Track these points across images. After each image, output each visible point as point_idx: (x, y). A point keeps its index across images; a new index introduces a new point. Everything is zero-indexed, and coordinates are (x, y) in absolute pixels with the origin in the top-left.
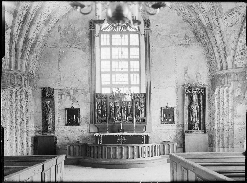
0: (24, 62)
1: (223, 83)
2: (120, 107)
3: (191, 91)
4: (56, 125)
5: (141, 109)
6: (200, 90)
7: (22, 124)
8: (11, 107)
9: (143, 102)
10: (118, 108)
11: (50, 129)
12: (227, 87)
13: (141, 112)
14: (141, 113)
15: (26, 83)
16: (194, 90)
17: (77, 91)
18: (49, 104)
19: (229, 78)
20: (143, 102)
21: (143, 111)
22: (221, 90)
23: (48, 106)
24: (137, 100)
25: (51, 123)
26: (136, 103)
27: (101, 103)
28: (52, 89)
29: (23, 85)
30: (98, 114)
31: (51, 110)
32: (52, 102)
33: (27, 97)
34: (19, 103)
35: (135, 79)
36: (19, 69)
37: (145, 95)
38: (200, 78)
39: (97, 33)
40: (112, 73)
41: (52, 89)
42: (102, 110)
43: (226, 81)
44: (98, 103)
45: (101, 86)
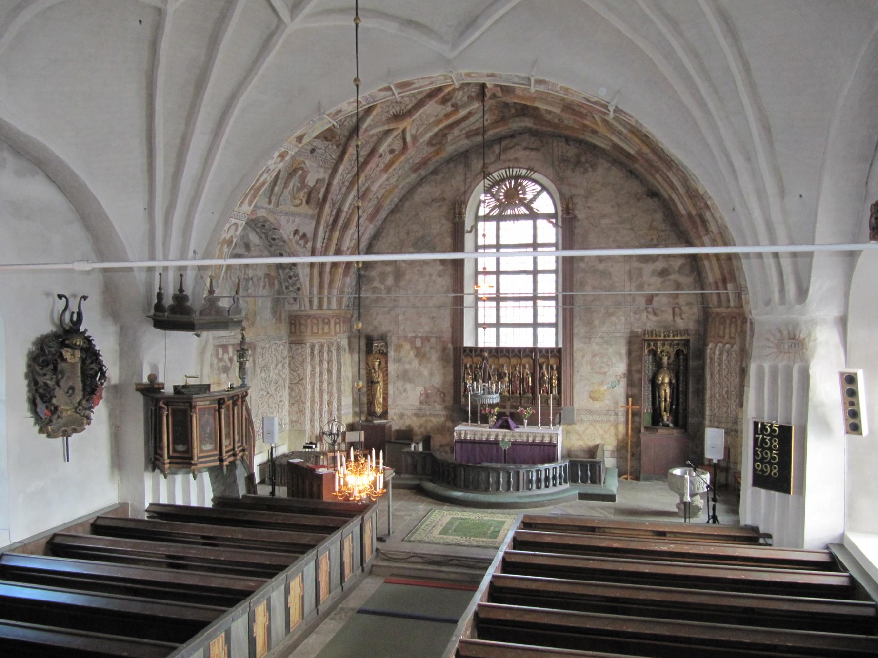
0: (335, 292)
1: (721, 333)
3: (656, 345)
4: (390, 402)
5: (551, 379)
6: (678, 344)
7: (330, 403)
8: (313, 375)
9: (555, 367)
11: (379, 410)
12: (728, 346)
13: (551, 385)
15: (338, 330)
16: (664, 345)
17: (429, 341)
18: (380, 364)
19: (733, 326)
20: (555, 367)
21: (555, 382)
22: (718, 348)
23: (376, 367)
24: (542, 360)
25: (381, 400)
26: (541, 368)
27: (471, 366)
28: (383, 338)
29: (333, 333)
31: (381, 375)
33: (338, 354)
34: (325, 365)
35: (548, 312)
36: (325, 306)
38: (681, 315)
39: (467, 227)
40: (498, 299)
41: (383, 338)
43: (727, 331)
44: (466, 366)
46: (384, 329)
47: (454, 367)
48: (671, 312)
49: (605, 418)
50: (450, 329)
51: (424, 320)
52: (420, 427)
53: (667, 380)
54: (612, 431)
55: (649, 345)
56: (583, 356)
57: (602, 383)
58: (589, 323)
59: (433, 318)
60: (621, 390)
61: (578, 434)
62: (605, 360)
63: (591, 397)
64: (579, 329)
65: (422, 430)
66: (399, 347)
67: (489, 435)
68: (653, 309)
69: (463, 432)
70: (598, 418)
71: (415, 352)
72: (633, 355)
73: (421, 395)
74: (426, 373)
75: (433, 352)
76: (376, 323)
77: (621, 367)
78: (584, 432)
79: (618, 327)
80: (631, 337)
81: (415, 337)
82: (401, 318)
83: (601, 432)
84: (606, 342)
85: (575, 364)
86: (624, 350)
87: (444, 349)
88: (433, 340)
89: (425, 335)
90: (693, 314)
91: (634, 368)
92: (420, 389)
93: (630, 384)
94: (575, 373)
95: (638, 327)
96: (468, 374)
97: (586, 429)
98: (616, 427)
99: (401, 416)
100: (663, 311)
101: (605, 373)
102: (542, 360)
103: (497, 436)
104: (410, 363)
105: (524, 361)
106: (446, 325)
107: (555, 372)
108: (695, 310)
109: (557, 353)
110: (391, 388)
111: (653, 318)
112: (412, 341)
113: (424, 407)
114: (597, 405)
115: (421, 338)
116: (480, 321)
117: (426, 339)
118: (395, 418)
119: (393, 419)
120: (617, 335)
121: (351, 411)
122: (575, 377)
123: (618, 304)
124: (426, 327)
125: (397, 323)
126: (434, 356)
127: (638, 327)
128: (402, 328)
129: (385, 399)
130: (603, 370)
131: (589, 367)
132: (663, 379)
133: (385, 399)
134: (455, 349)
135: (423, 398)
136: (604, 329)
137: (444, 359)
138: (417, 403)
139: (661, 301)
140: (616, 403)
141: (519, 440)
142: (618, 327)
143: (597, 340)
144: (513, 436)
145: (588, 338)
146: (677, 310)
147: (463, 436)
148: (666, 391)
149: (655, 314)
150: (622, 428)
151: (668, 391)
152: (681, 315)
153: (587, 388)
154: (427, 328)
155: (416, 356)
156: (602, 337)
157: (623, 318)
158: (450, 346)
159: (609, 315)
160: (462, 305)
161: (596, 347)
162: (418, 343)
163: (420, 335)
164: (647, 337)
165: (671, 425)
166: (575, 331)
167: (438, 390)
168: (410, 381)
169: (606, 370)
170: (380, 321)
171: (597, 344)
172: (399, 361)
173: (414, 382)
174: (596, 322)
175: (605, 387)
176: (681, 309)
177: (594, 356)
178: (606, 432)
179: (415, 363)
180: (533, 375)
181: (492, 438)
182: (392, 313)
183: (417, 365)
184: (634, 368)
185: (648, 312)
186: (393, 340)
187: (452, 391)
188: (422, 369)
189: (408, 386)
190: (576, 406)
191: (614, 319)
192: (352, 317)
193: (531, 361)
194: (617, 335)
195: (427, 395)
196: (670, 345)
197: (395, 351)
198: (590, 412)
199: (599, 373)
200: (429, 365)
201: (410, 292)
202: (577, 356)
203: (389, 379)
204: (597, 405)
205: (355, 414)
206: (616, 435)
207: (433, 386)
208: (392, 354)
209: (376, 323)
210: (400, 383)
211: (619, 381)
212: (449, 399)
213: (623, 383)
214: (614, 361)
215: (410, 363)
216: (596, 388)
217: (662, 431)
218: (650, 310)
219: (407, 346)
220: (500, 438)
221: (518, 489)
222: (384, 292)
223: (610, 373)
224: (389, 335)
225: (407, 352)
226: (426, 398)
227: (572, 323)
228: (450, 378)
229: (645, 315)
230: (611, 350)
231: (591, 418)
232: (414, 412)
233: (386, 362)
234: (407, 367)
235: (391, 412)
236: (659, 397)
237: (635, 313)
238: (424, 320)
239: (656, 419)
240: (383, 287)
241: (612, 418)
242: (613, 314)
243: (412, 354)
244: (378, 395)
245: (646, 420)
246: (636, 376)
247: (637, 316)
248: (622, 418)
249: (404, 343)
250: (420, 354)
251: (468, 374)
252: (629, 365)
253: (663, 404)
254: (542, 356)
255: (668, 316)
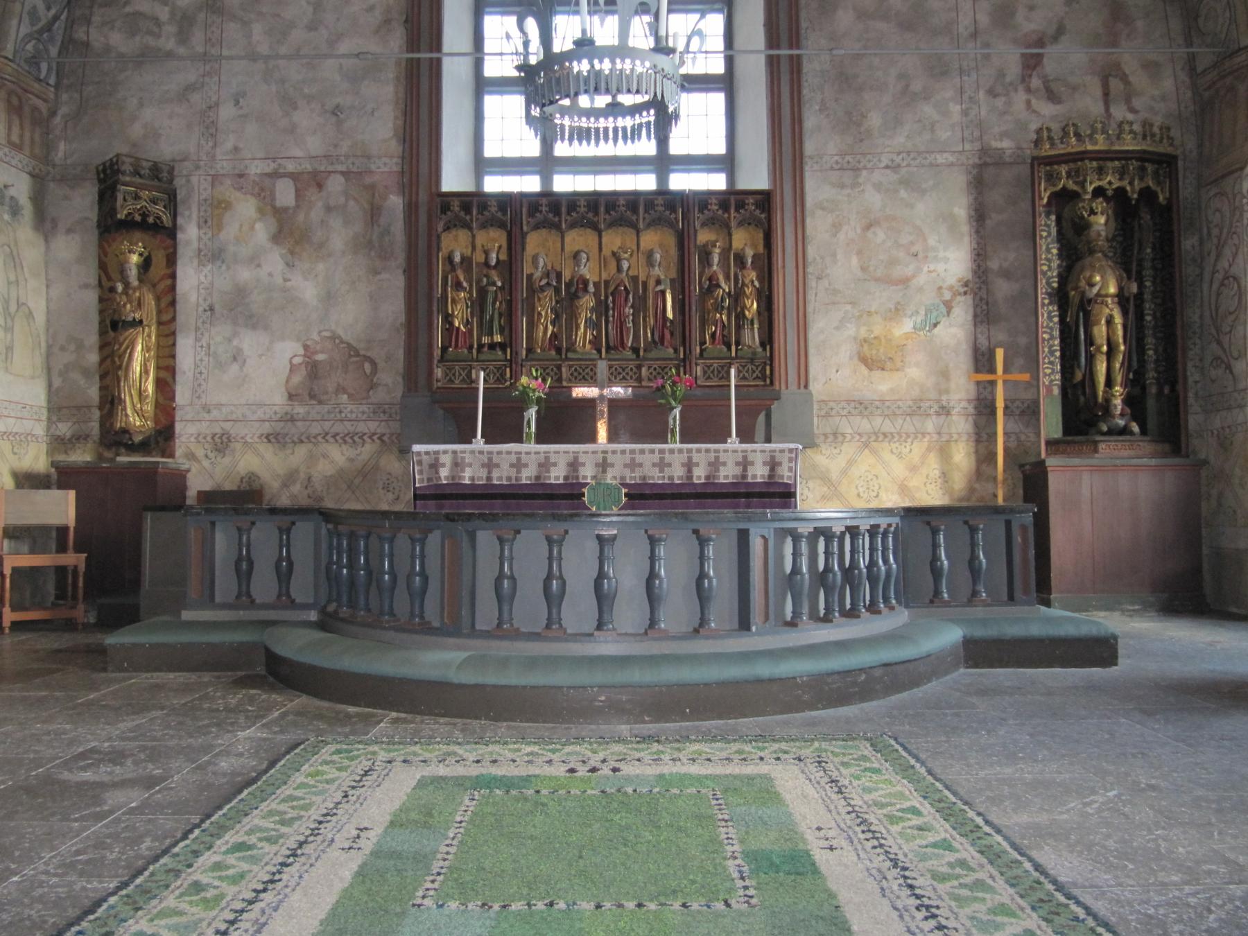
2: (596, 285)
5: (737, 296)
9: (749, 253)
10: (585, 290)
13: (740, 317)
14: (739, 328)
16: (1101, 171)
17: (320, 186)
18: (146, 265)
20: (749, 253)
23: (133, 273)
25: (150, 387)
28: (162, 179)
30: (449, 328)
31: (150, 300)
32: (159, 259)
35: (701, 125)
37: (765, 200)
38: (1128, 100)
41: (162, 179)
42: (479, 304)
44: (450, 259)
45: (482, 165)
46: (165, 151)
47: (411, 272)
48: (1098, 92)
49: (909, 427)
50: (395, 147)
51: (305, 118)
52: (290, 478)
53: (1112, 290)
54: (933, 467)
55: (1051, 178)
56: (836, 227)
57: (897, 312)
58: (852, 122)
59: (336, 111)
60: (955, 331)
61: (825, 479)
62: (905, 239)
63: (865, 361)
64: (821, 142)
65: (296, 488)
66: (216, 211)
67: (545, 465)
68: (1046, 82)
69: (446, 460)
70: (888, 427)
71: (272, 223)
72: (993, 219)
73: (293, 369)
74: (309, 291)
75: (336, 222)
76: (136, 130)
77: (952, 262)
78: (844, 472)
79: (944, 135)
80: (982, 166)
81: (275, 175)
82: (227, 112)
83: (899, 469)
84: (905, 183)
85: (811, 252)
86: (961, 210)
87: (374, 213)
88: (336, 184)
89: (308, 167)
90: (1163, 98)
91: (994, 264)
92: (288, 351)
93: (984, 314)
94: (812, 283)
95: (1004, 135)
96: (458, 286)
97: (851, 463)
98: (944, 452)
99: (222, 444)
100: (1074, 88)
101: (905, 281)
102: (704, 236)
103: (574, 465)
104: (254, 260)
105: (650, 239)
106: (380, 131)
107: (753, 275)
108: (1168, 84)
109: (755, 210)
110: (187, 353)
111: (1047, 110)
112: (263, 192)
113: (300, 410)
114: (883, 385)
115: (294, 177)
116: (490, 151)
117: (310, 181)
118: (200, 453)
119: (191, 456)
120: (941, 159)
121: (40, 430)
122: (811, 296)
123: (938, 69)
124: (310, 142)
125: (211, 130)
126: (339, 236)
127: (1004, 135)
128: (229, 145)
129: (165, 386)
130: (898, 272)
131: (854, 261)
132: (1105, 284)
133: (165, 386)
134: (411, 209)
135: (297, 379)
136: (900, 140)
137: (370, 245)
138: (279, 398)
139: (1069, 58)
140: (945, 374)
141: (656, 477)
142: (944, 135)
143: (877, 176)
144: (633, 465)
145: (850, 169)
146: (1115, 84)
147: (444, 473)
148: (1109, 324)
149: (1052, 96)
150: (962, 456)
151: (1118, 320)
152: (1128, 100)
153: (851, 330)
154: (315, 145)
155: (276, 238)
156: (893, 167)
157: (956, 109)
158: (396, 202)
159: (908, 97)
160: (438, 48)
161: (874, 199)
162: (285, 194)
163: (291, 167)
164: (1046, 150)
165: (1135, 428)
166: (809, 147)
167: (352, 350)
168: (254, 322)
169: (909, 270)
170: (156, 122)
171: (878, 187)
172: (214, 255)
173: (266, 328)
174: (875, 120)
175: (907, 326)
176: (1124, 79)
177: (869, 227)
178: (913, 469)
179: (274, 262)
180: (681, 286)
181: (557, 475)
182: (195, 97)
183: (280, 266)
184: (994, 264)
185: (1028, 90)
186: (195, 188)
187: (400, 354)
188: (297, 281)
189: (249, 342)
190: (816, 387)
191: (928, 110)
192: (53, 113)
193: (671, 241)
194: (941, 159)
195: (314, 370)
196: (1122, 174)
197: (203, 223)
198: (862, 407)
199: (888, 281)
200: (321, 267)
201: (257, 29)
202: (817, 226)
203: (181, 318)
204: (883, 385)
205: (58, 443)
206: (944, 475)
207: (334, 337)
208: (190, 233)
209: (136, 130)
210: (219, 333)
211: (949, 306)
212: (391, 381)
213: (962, 312)
214: (932, 241)
215: (254, 260)
216: (878, 330)
217: (1108, 449)
218: (1036, 82)
219: (246, 208)
220: (587, 473)
221: (744, 624)
222: (170, 29)
223: (922, 279)
224: (182, 169)
225: (246, 222)
226: (311, 381)
227: (797, 121)
228: (394, 308)
229: (1020, 97)
230: (923, 208)
231: (865, 425)
232: (267, 429)
233: (171, 260)
234: (245, 274)
235: (186, 432)
236: (1090, 341)
237: (992, 93)
238: (305, 118)
239: (1082, 420)
240: (163, 13)
241: (930, 426)
242: (926, 96)
243: (262, 233)
244: (136, 367)
245: (1051, 423)
246: (1003, 289)
247: (1000, 102)
248: (961, 425)
249: (234, 196)
250: (290, 233)
251: (458, 286)
252: (980, 256)
253: (1101, 368)
254: (710, 223)
255: (1089, 104)
